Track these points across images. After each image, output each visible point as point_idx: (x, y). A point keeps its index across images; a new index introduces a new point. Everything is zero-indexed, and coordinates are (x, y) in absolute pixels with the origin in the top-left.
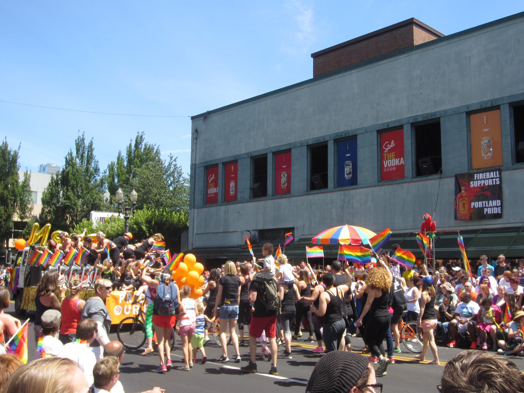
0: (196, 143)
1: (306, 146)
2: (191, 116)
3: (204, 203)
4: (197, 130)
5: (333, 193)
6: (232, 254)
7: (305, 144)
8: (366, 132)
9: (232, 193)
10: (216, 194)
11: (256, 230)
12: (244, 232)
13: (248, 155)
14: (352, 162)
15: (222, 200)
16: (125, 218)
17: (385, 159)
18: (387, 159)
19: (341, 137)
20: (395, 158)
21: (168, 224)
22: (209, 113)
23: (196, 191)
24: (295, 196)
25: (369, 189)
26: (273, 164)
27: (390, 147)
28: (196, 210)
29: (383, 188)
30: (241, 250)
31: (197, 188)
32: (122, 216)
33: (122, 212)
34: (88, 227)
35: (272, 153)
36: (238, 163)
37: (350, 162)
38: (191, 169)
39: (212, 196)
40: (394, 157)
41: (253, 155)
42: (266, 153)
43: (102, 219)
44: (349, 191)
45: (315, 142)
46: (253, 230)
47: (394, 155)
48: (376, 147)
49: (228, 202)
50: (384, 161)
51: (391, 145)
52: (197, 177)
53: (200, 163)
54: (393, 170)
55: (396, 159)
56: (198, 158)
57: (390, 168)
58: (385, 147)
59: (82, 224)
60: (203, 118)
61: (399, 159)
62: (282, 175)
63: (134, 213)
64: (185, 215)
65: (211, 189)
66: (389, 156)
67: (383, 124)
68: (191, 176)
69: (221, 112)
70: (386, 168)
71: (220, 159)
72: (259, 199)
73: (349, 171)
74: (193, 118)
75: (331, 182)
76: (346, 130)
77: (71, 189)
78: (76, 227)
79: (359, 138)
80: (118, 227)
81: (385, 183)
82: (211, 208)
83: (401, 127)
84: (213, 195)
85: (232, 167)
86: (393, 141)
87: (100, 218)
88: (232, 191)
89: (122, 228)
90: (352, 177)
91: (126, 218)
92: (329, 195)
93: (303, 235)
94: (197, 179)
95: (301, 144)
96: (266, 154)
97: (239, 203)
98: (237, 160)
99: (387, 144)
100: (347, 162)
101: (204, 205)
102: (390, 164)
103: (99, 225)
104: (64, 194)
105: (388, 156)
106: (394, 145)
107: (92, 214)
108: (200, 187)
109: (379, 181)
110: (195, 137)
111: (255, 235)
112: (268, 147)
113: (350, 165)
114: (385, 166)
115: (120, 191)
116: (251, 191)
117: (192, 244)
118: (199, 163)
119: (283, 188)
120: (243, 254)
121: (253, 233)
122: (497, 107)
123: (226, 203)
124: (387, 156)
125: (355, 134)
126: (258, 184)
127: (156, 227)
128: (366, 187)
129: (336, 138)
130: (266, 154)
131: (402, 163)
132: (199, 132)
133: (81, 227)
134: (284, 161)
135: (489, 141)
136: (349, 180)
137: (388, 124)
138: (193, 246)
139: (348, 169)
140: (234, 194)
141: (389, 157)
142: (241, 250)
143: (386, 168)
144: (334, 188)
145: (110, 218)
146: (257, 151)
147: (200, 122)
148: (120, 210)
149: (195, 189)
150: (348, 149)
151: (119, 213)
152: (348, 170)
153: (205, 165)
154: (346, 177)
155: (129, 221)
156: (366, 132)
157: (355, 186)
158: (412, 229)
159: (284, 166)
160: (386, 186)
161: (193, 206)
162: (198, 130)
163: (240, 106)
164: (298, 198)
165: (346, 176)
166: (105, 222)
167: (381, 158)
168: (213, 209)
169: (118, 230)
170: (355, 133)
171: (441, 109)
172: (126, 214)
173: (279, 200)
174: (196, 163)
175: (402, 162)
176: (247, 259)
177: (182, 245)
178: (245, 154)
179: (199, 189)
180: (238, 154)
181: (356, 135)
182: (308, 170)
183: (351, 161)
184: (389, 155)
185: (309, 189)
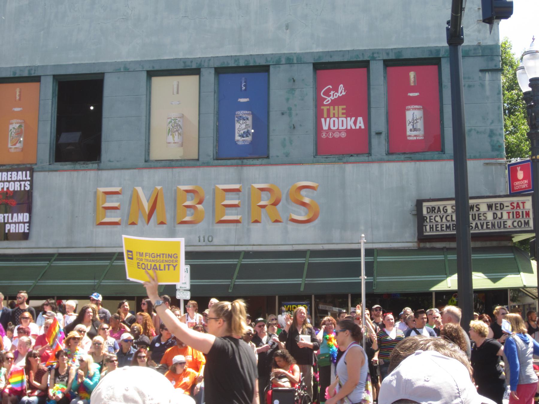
5: (123, 171)
14: (253, 114)
17: (325, 115)
18: (329, 116)
20: (345, 116)
27: (334, 95)
40: (343, 114)
42: (102, 72)
47: (344, 111)
48: (50, 103)
50: (323, 120)
51: (337, 92)
54: (340, 136)
55: (349, 119)
57: (334, 132)
58: (324, 94)
61: (353, 119)
66: (334, 112)
70: (327, 132)
73: (246, 130)
76: (37, 65)
82: (245, 168)
83: (365, 64)
86: (342, 85)
88: (415, 130)
90: (252, 143)
92: (375, 167)
99: (329, 90)
100: (240, 113)
102: (334, 126)
105: (332, 112)
106: (344, 93)
113: (248, 119)
114: (325, 128)
119: (12, 151)
122: (196, 72)
124: (328, 110)
129: (316, 62)
131: (360, 127)
135: (20, 126)
136: (242, 146)
137: (399, 51)
139: (243, 126)
140: (422, 138)
141: (334, 114)
143: (327, 132)
146: (418, 48)
154: (238, 141)
158: (403, 242)
159: (17, 109)
165: (237, 138)
167: (319, 115)
171: (389, 48)
175: (361, 123)
180: (361, 48)
183: (249, 112)
184: (334, 109)
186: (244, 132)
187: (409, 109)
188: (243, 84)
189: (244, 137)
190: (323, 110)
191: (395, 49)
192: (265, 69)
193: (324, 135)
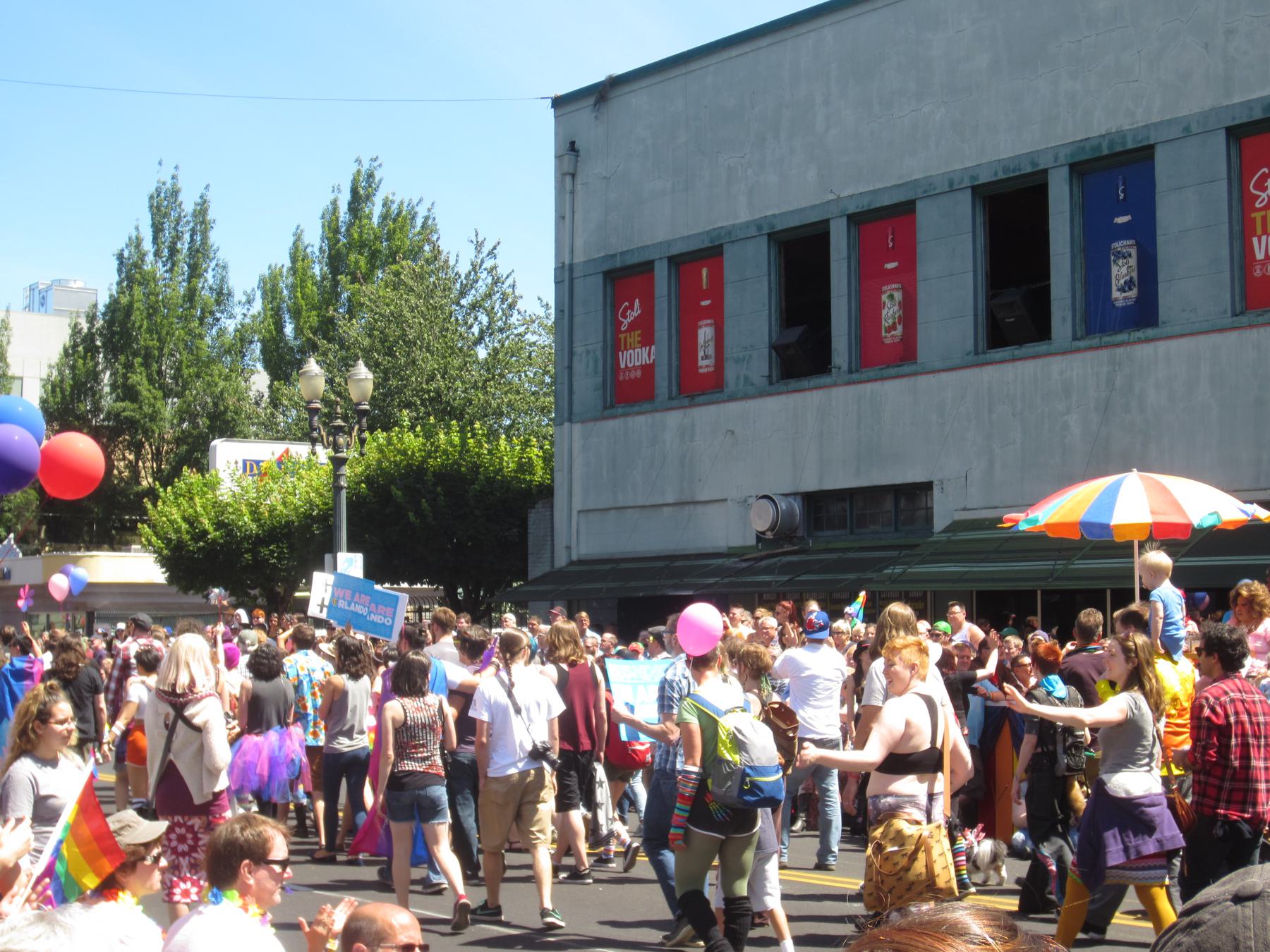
0: (572, 192)
1: (969, 192)
2: (553, 95)
3: (605, 401)
4: (573, 143)
6: (711, 581)
7: (967, 183)
8: (1187, 132)
9: (705, 364)
10: (648, 370)
11: (795, 494)
12: (750, 501)
13: (760, 228)
14: (1139, 246)
15: (670, 392)
16: (332, 459)
17: (1259, 231)
19: (1097, 155)
21: (482, 477)
22: (615, 83)
23: (575, 359)
24: (933, 372)
25: (1202, 338)
26: (849, 258)
28: (577, 428)
29: (1254, 335)
30: (744, 565)
31: (579, 348)
32: (323, 454)
33: (322, 442)
34: (205, 493)
35: (845, 219)
36: (726, 256)
37: (1130, 246)
38: (556, 283)
39: (633, 375)
41: (779, 227)
43: (250, 466)
44: (1128, 348)
45: (1001, 176)
46: (786, 495)
49: (692, 397)
50: (1255, 240)
52: (578, 310)
53: (594, 260)
56: (579, 242)
58: (1256, 187)
59: (182, 484)
60: (592, 101)
62: (884, 298)
63: (362, 442)
64: (541, 448)
65: (631, 351)
67: (1248, 105)
68: (559, 310)
69: (657, 78)
71: (660, 243)
72: (805, 383)
74: (558, 102)
75: (1064, 319)
76: (1114, 130)
77: (142, 365)
78: (162, 494)
79: (1160, 156)
80: (308, 493)
81: (1260, 318)
82: (630, 419)
84: (639, 373)
85: (705, 272)
87: (245, 462)
88: (706, 357)
89: (321, 495)
90: (1138, 300)
91: (338, 462)
92: (1057, 365)
93: (964, 509)
94: (577, 320)
95: (951, 183)
96: (827, 221)
97: (732, 398)
98: (721, 246)
100: (1118, 245)
101: (605, 408)
103: (242, 488)
104: (115, 382)
107: (215, 447)
108: (590, 347)
109: (1238, 311)
110: (567, 168)
111: (790, 513)
112: (832, 197)
113: (1130, 255)
115: (312, 366)
116: (774, 353)
117: (568, 548)
118: (585, 262)
119: (888, 341)
120: (750, 579)
121: (783, 505)
123: (686, 402)
125: (1145, 143)
126: (795, 334)
127: (439, 489)
128: (1191, 334)
129: (1076, 159)
130: (827, 221)
132: (581, 153)
133: (180, 495)
134: (891, 245)
136: (1123, 307)
138: (570, 555)
139: (1124, 270)
140: (711, 369)
142: (744, 565)
143: (1263, 265)
144: (1075, 338)
145: (280, 462)
147: (584, 113)
148: (315, 434)
149: (571, 353)
150: (1122, 196)
151: (314, 442)
152: (1122, 271)
153: (606, 267)
154: (1116, 299)
155: (346, 470)
156: (1187, 132)
157: (1150, 332)
159: (891, 266)
160: (1262, 330)
161: (567, 413)
162: (577, 145)
163: (725, 55)
164: (944, 376)
165: (1116, 294)
166: (262, 475)
168: (639, 423)
169: (310, 502)
170: (1148, 138)
172: (336, 448)
173: (876, 386)
174: (576, 261)
176: (765, 597)
177: (531, 549)
178: (747, 225)
179: (588, 352)
180: (725, 224)
181: (1150, 149)
182: (979, 277)
183: (1132, 242)
185: (982, 344)
186: (1125, 282)
187: (701, 327)
188: (890, 237)
189: (1125, 292)
190: (1255, 218)
191: (1262, 98)
192: (905, 210)
193: (1258, 271)
